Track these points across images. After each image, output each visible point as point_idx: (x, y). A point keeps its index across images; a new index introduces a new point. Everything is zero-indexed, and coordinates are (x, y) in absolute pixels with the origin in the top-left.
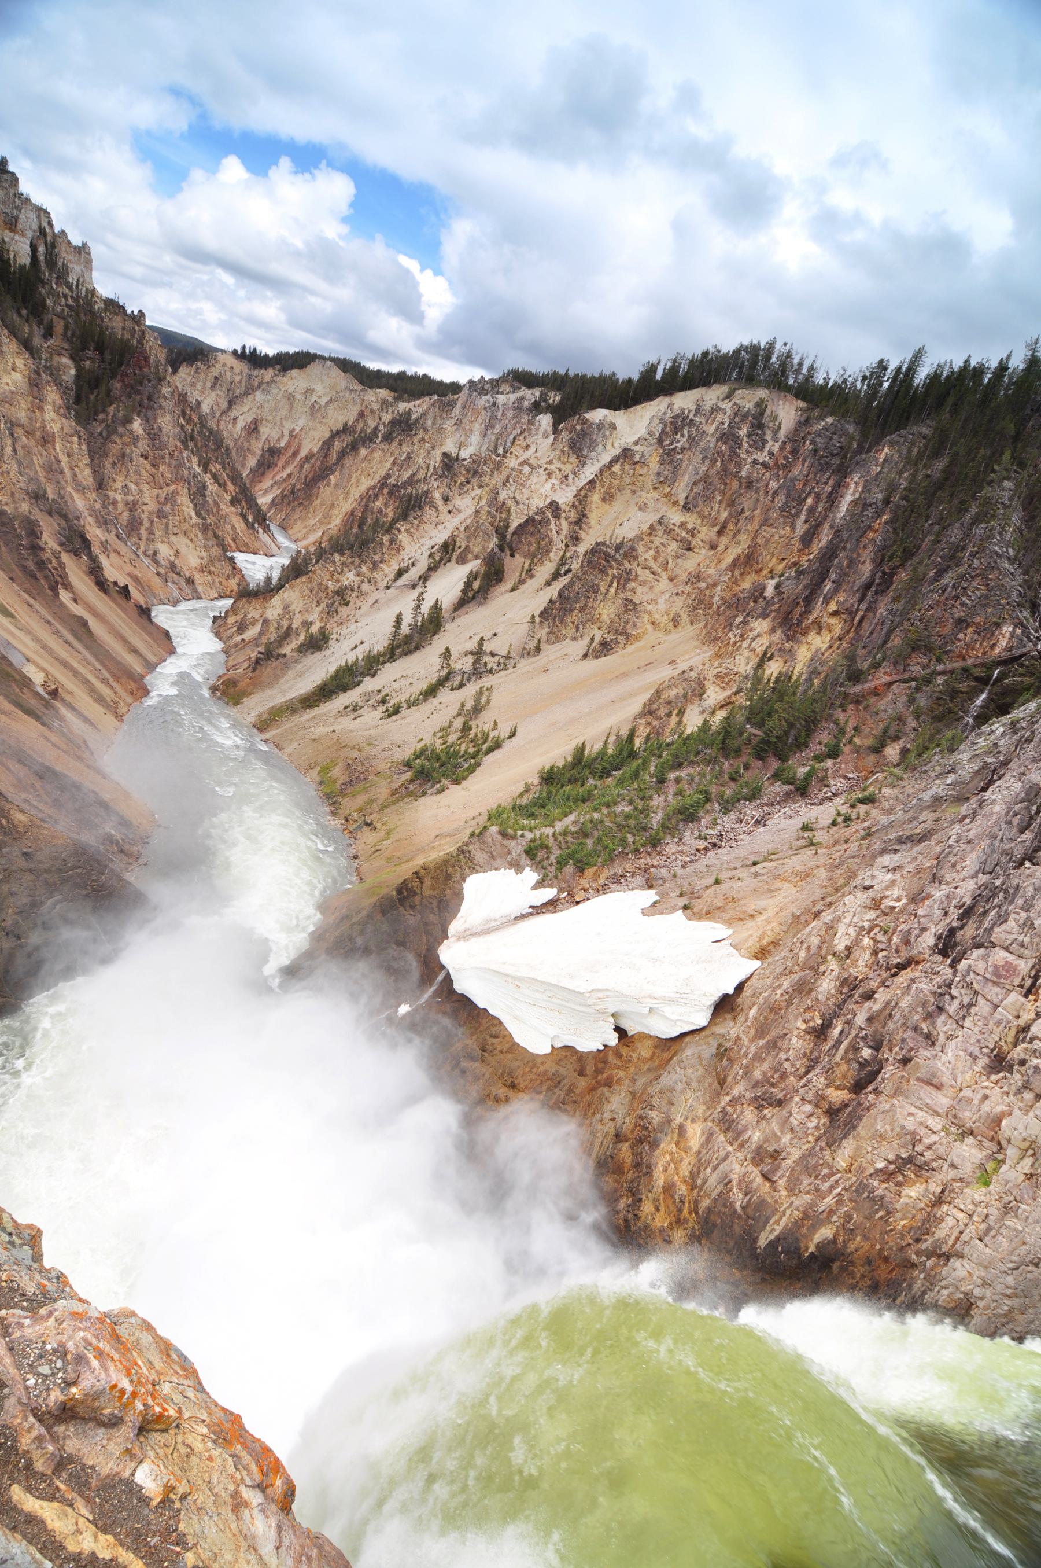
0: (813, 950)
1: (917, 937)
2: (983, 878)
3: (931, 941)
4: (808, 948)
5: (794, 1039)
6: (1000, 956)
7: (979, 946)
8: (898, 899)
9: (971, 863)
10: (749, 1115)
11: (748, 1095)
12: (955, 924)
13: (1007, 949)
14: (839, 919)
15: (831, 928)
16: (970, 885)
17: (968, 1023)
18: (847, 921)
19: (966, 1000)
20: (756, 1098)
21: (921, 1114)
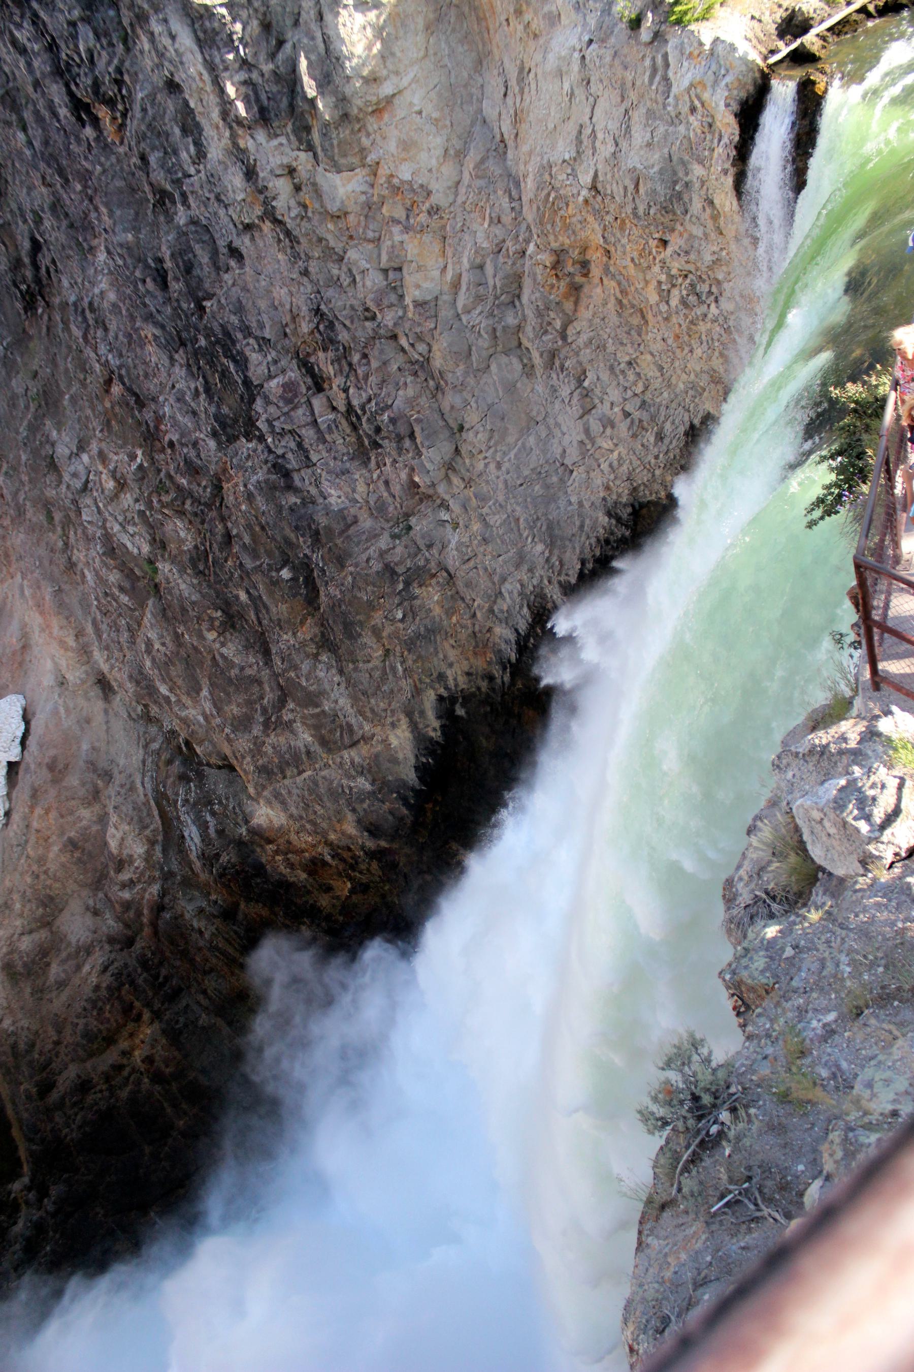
0: (127, 585)
1: (198, 456)
2: (180, 357)
3: (212, 444)
4: (121, 589)
5: (224, 650)
6: (273, 385)
7: (252, 400)
8: (133, 457)
9: (154, 354)
10: (276, 740)
11: (257, 730)
12: (212, 409)
13: (271, 377)
14: (108, 537)
15: (112, 550)
16: (179, 372)
17: (314, 457)
18: (117, 528)
19: (293, 445)
20: (266, 724)
21: (371, 551)
